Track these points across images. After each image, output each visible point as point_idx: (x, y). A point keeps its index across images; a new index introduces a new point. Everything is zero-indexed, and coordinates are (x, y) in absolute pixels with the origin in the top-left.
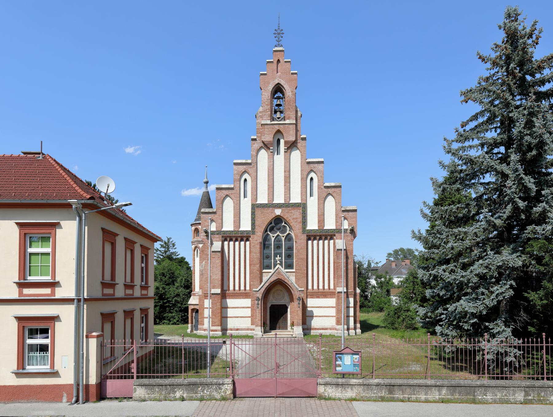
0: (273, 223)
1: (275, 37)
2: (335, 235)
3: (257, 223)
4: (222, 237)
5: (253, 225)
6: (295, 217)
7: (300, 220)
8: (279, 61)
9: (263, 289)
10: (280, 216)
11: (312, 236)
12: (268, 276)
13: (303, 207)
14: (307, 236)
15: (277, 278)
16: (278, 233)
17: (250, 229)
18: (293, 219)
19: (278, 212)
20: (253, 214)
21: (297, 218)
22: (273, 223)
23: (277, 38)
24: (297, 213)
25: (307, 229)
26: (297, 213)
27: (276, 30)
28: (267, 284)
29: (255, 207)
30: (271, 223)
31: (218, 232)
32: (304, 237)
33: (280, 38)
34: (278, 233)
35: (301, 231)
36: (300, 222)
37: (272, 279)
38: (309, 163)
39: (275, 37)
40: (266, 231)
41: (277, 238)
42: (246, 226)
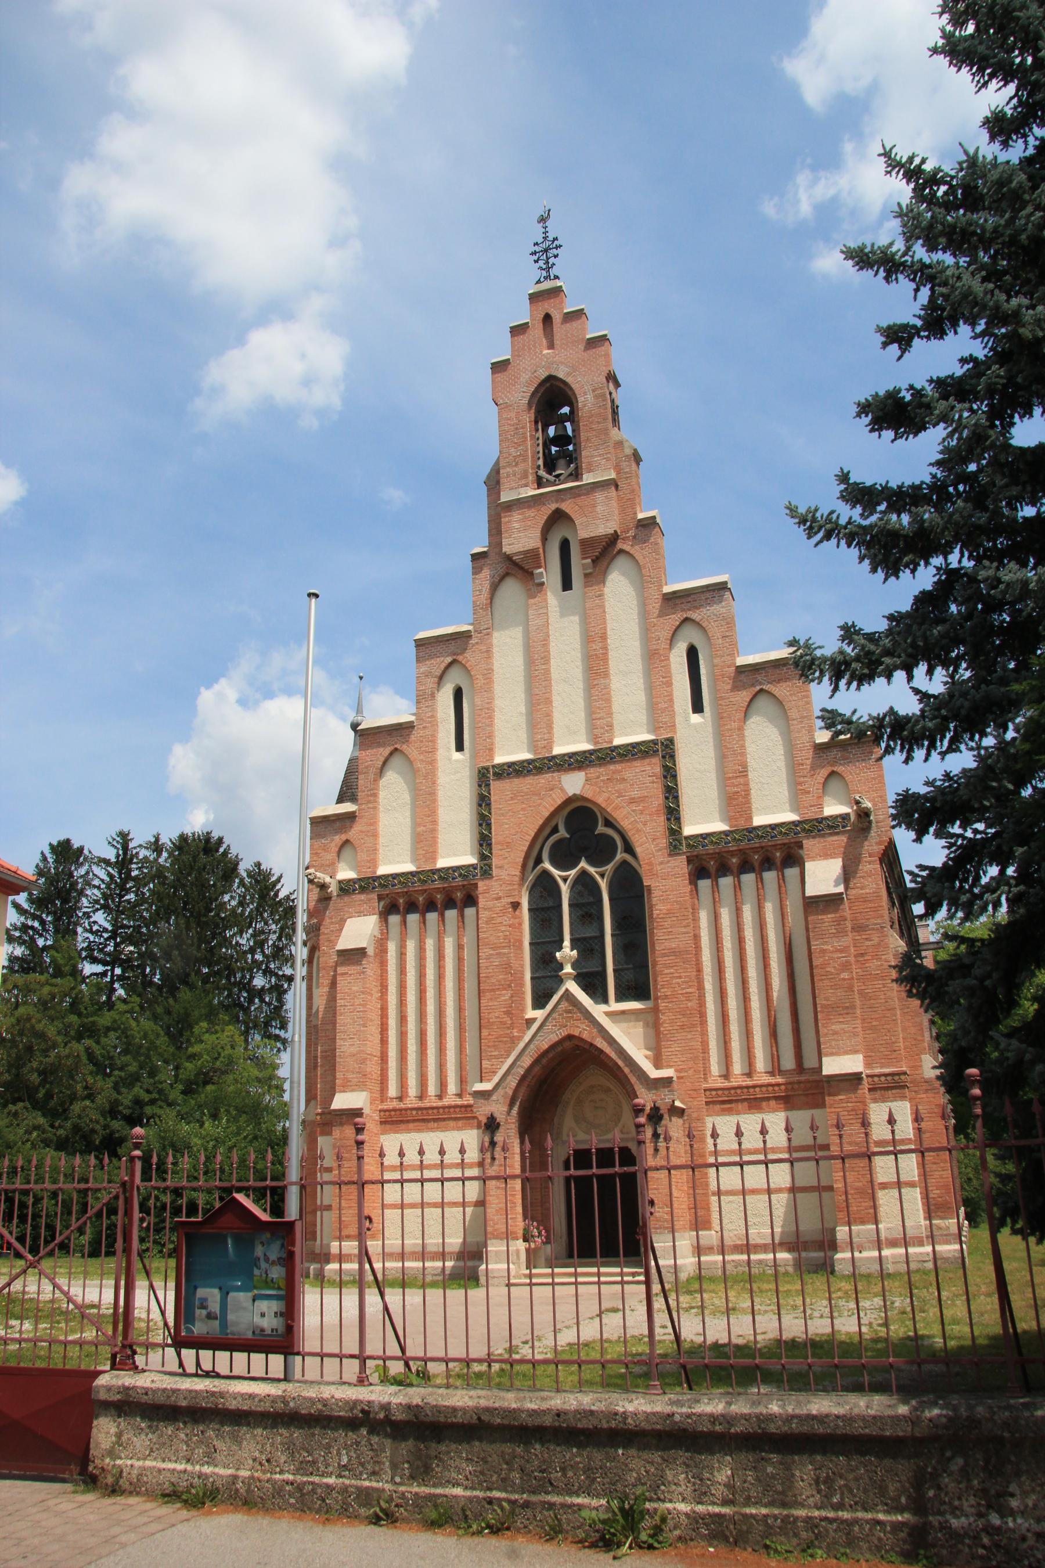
0: (562, 828)
1: (536, 262)
2: (800, 846)
3: (497, 835)
4: (380, 898)
5: (484, 841)
6: (635, 793)
7: (657, 799)
8: (547, 319)
9: (513, 1082)
10: (582, 798)
11: (713, 862)
12: (538, 1027)
13: (663, 751)
14: (689, 861)
15: (564, 1033)
16: (583, 864)
17: (471, 860)
18: (632, 801)
19: (574, 783)
20: (483, 801)
21: (642, 799)
22: (562, 828)
23: (541, 263)
24: (644, 775)
25: (688, 830)
26: (644, 775)
27: (536, 244)
28: (527, 1061)
29: (486, 777)
30: (555, 830)
31: (366, 884)
32: (680, 865)
33: (551, 261)
34: (583, 864)
35: (663, 842)
36: (657, 812)
37: (544, 1043)
38: (673, 600)
39: (536, 262)
40: (539, 860)
41: (585, 884)
42: (456, 853)
